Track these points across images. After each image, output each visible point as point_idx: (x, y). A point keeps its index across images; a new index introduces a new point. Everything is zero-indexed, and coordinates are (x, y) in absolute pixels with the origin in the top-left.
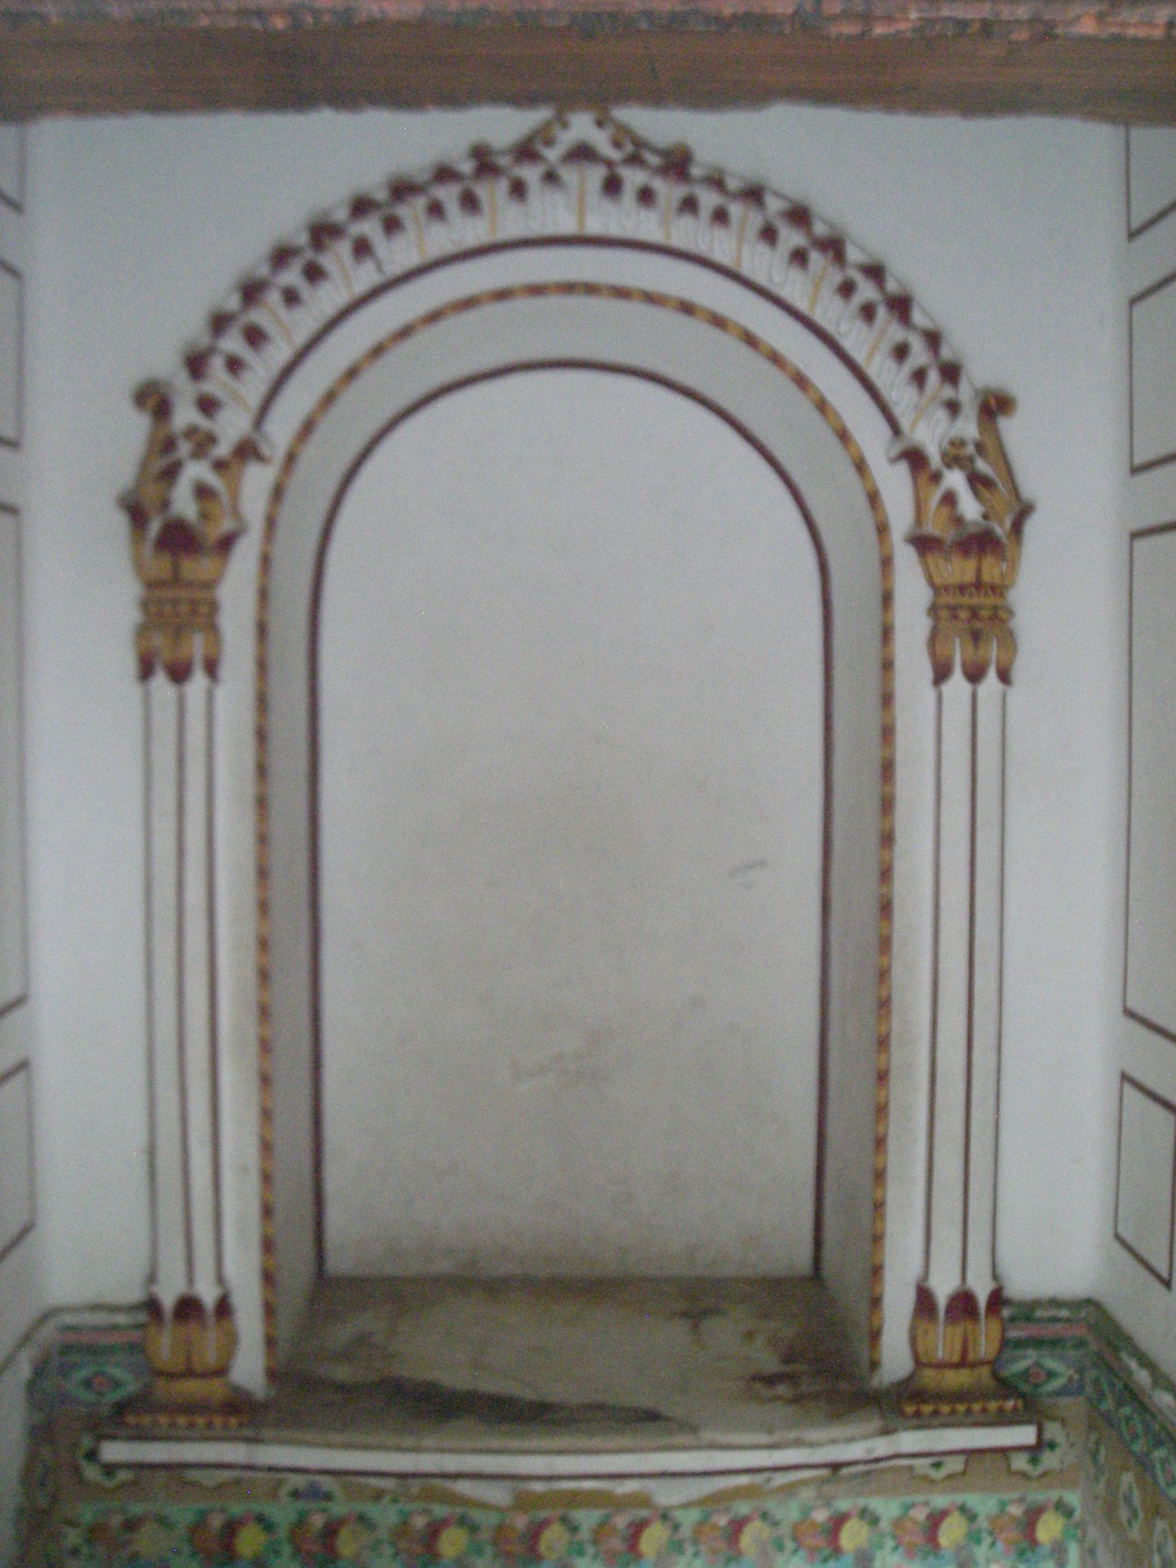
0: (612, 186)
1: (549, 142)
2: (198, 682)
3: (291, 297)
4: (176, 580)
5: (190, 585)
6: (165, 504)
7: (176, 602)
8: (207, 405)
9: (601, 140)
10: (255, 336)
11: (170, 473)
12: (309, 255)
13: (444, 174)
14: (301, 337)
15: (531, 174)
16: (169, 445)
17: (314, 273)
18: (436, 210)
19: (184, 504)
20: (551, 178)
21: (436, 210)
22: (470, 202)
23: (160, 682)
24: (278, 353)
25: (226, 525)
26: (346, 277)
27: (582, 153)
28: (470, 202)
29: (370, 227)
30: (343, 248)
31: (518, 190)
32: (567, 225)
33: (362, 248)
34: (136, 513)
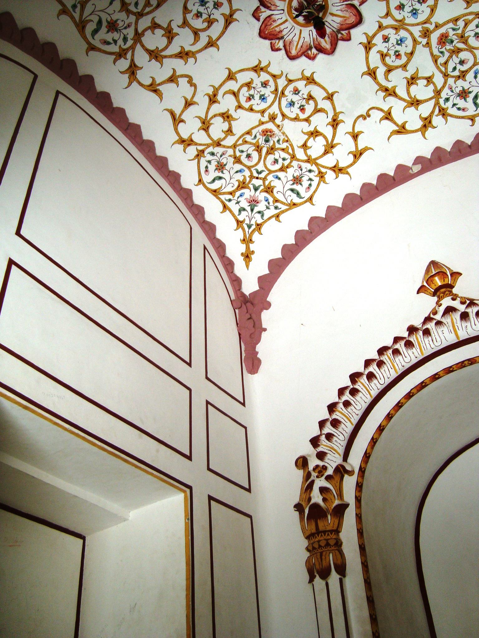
0: (465, 316)
1: (435, 313)
2: (334, 577)
3: (347, 404)
4: (318, 532)
5: (324, 532)
6: (310, 499)
7: (319, 541)
8: (321, 456)
9: (456, 304)
10: (335, 423)
11: (309, 487)
12: (352, 387)
13: (397, 340)
14: (355, 419)
15: (431, 326)
16: (309, 475)
17: (354, 392)
18: (396, 352)
19: (317, 498)
20: (439, 323)
21: (396, 352)
22: (409, 344)
23: (318, 579)
24: (347, 428)
25: (337, 502)
26: (367, 391)
27: (450, 310)
28: (409, 344)
29: (373, 368)
30: (364, 379)
31: (427, 332)
32: (452, 339)
33: (371, 376)
34: (299, 507)
